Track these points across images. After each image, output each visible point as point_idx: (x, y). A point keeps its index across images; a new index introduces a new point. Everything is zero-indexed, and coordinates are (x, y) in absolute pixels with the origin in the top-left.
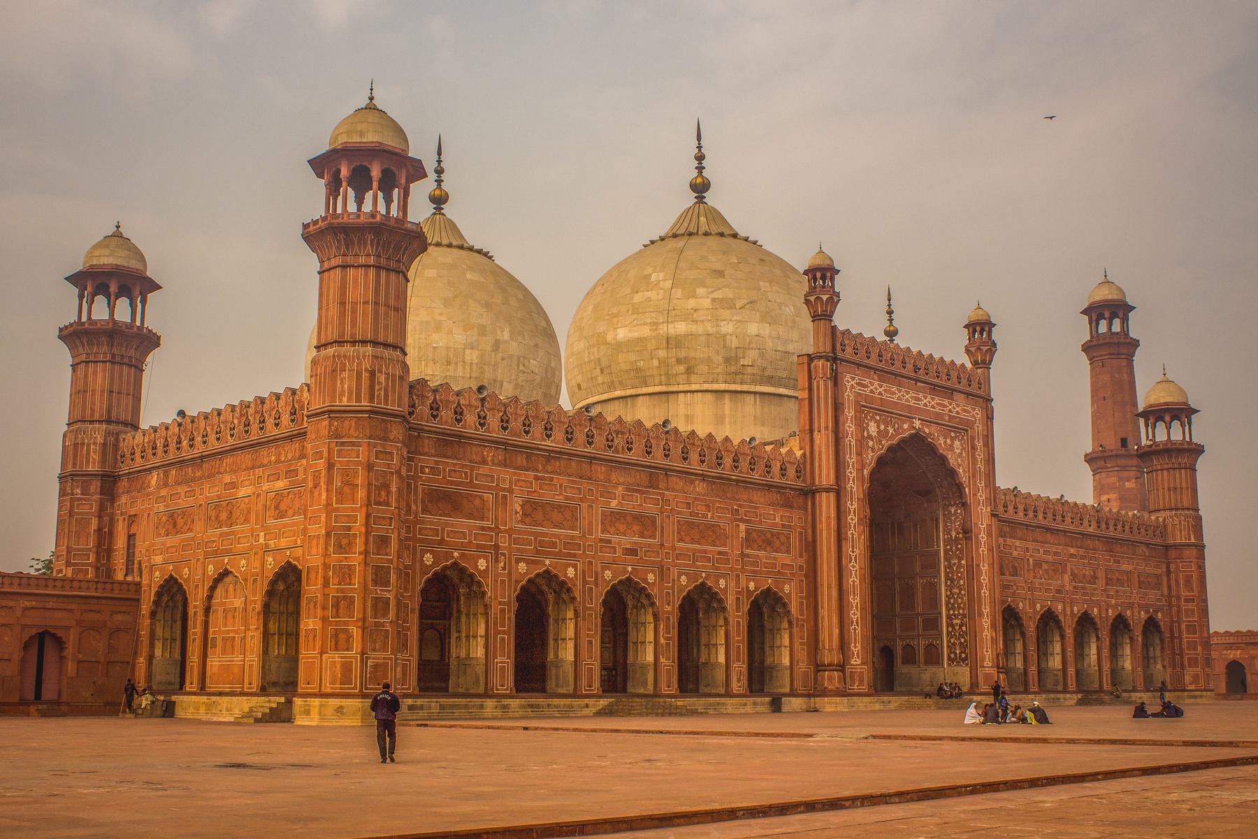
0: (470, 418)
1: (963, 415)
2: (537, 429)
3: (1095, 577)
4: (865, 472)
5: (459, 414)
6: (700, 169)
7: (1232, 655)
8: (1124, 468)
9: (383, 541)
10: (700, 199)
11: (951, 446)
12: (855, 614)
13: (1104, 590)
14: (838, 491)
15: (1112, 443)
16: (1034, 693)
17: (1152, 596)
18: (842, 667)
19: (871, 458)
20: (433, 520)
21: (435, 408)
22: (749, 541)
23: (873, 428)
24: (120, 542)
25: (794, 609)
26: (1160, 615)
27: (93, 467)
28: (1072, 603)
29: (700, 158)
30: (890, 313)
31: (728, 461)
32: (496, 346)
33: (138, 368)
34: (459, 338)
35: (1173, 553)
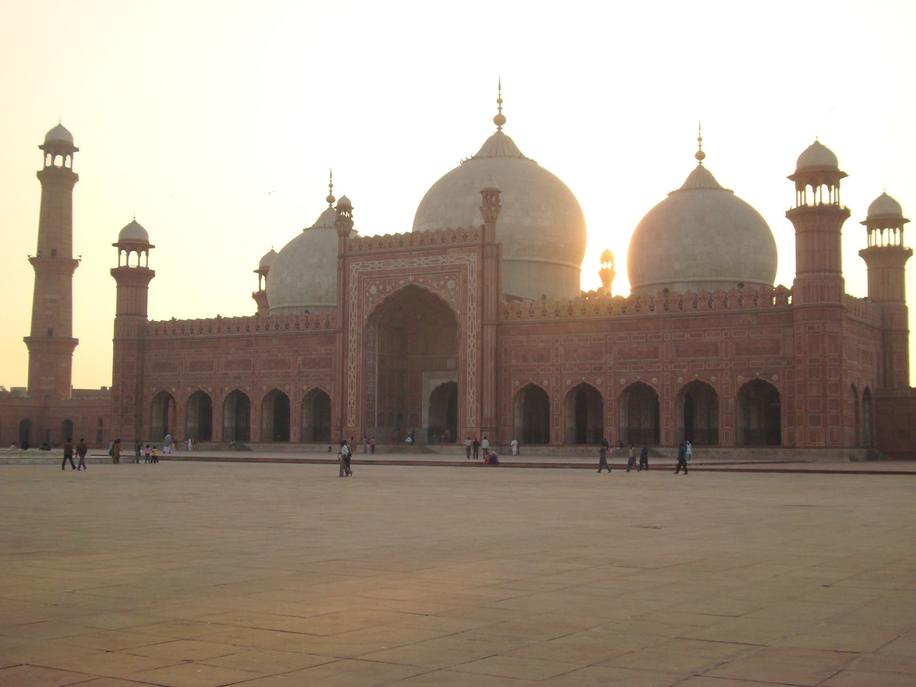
0: (170, 332)
1: (457, 262)
4: (365, 317)
5: (165, 331)
6: (500, 109)
10: (499, 129)
11: (445, 286)
12: (351, 399)
13: (671, 362)
14: (344, 330)
16: (558, 446)
18: (341, 429)
19: (371, 307)
23: (373, 290)
29: (500, 101)
30: (700, 139)
31: (292, 325)
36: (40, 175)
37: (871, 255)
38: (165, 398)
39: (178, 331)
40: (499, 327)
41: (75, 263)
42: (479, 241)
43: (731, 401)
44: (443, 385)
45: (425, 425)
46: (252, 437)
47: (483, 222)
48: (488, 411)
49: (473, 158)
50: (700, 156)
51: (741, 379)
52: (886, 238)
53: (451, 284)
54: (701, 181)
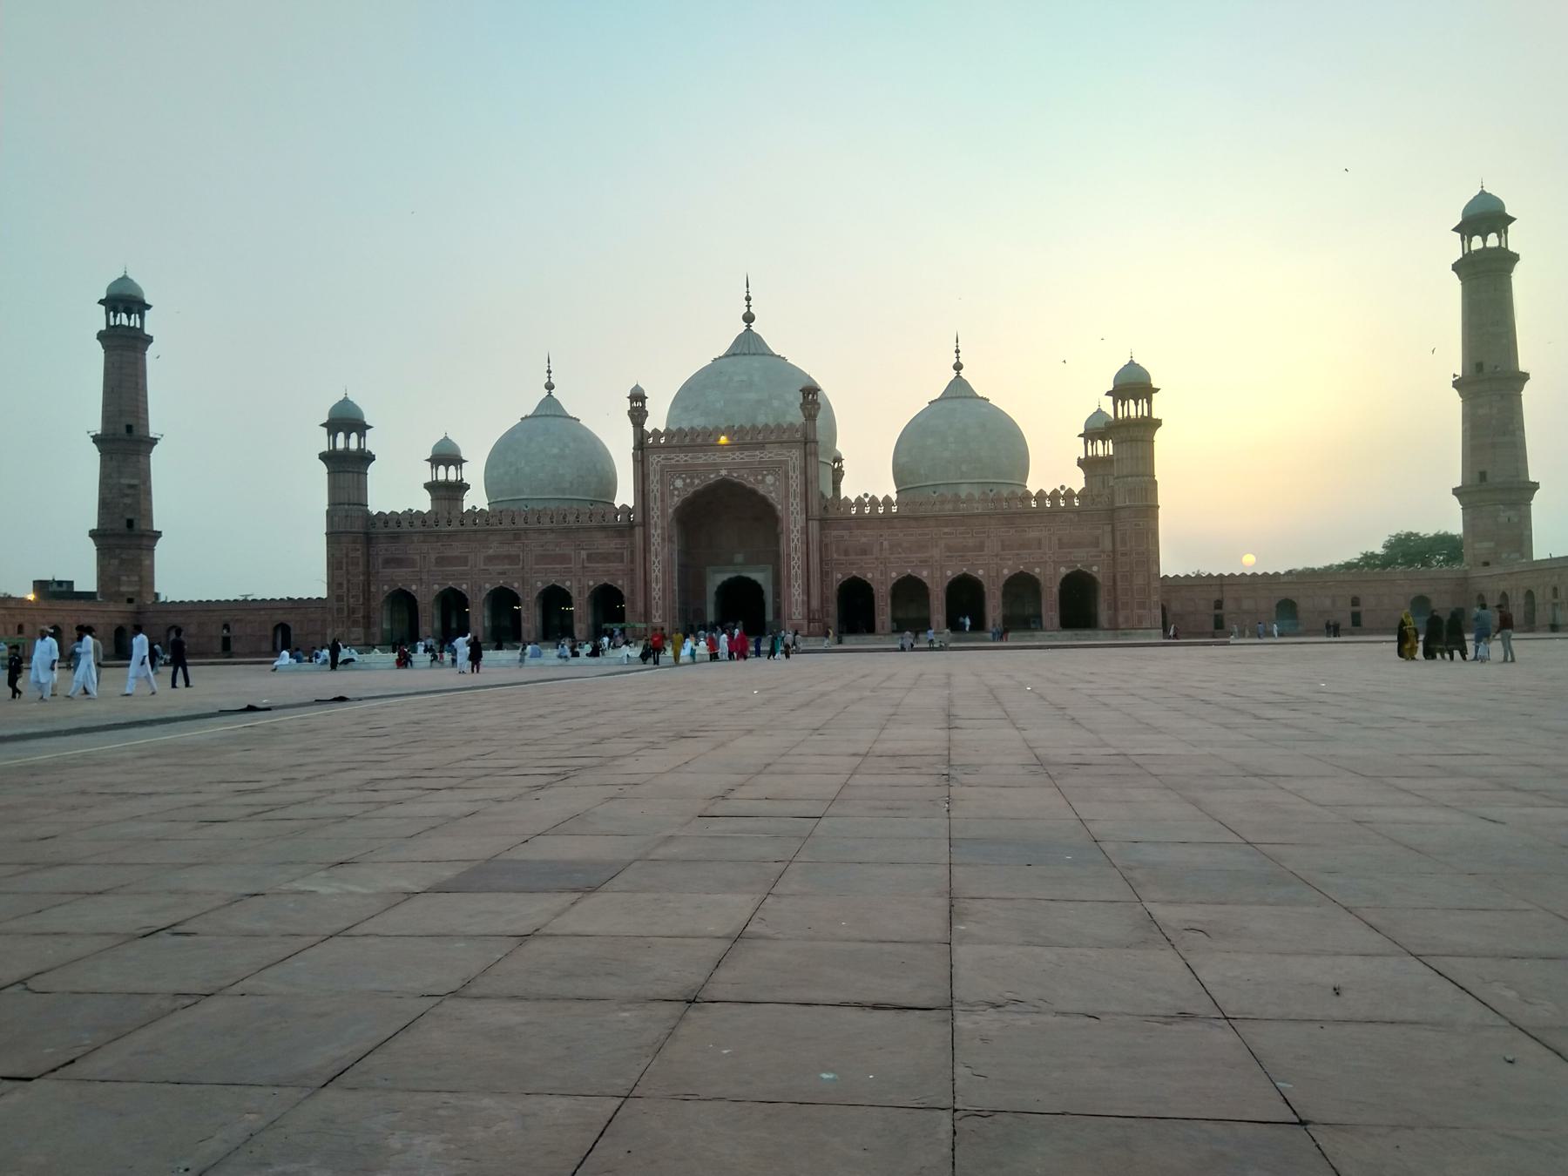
0: (405, 524)
3: (981, 547)
5: (399, 524)
7: (1503, 586)
9: (340, 585)
11: (763, 481)
14: (645, 523)
19: (677, 501)
22: (590, 558)
23: (679, 483)
25: (626, 593)
26: (1095, 569)
29: (748, 299)
31: (571, 519)
32: (517, 471)
36: (101, 336)
37: (1086, 464)
38: (404, 601)
39: (417, 523)
40: (824, 523)
41: (154, 441)
42: (798, 436)
43: (1056, 590)
44: (730, 580)
45: (711, 617)
46: (524, 636)
47: (803, 419)
48: (815, 603)
49: (726, 356)
50: (958, 367)
51: (1064, 571)
52: (1102, 449)
53: (770, 479)
54: (959, 390)
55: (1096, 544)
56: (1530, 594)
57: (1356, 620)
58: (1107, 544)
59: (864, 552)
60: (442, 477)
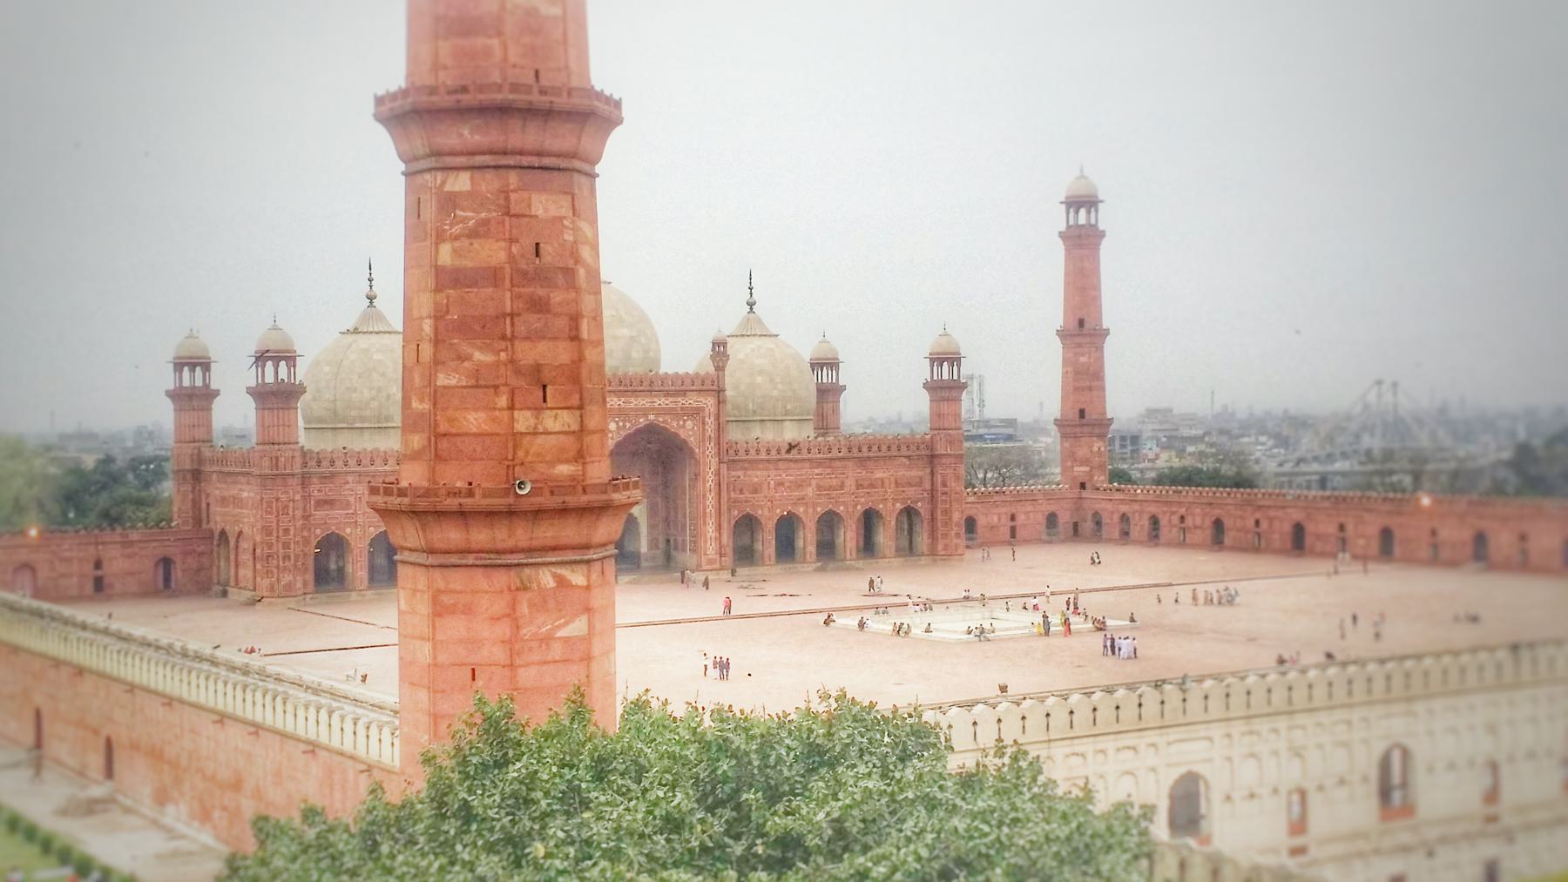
0: (339, 463)
2: (379, 461)
3: (842, 486)
5: (332, 463)
8: (1079, 346)
9: (286, 531)
11: (683, 426)
15: (1073, 325)
17: (911, 492)
20: (319, 514)
21: (319, 463)
24: (204, 505)
27: (188, 467)
28: (815, 505)
33: (209, 409)
34: (367, 394)
35: (936, 461)
39: (352, 462)
48: (725, 539)
51: (899, 506)
52: (826, 377)
53: (689, 424)
55: (920, 483)
56: (1155, 521)
57: (1013, 535)
58: (927, 486)
59: (756, 490)
60: (186, 383)
